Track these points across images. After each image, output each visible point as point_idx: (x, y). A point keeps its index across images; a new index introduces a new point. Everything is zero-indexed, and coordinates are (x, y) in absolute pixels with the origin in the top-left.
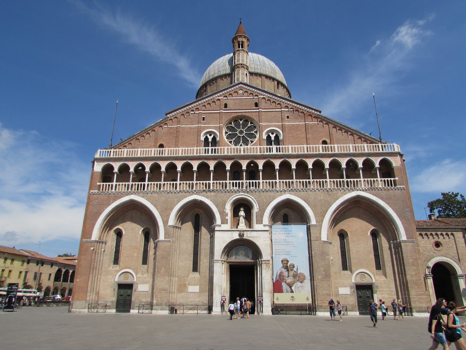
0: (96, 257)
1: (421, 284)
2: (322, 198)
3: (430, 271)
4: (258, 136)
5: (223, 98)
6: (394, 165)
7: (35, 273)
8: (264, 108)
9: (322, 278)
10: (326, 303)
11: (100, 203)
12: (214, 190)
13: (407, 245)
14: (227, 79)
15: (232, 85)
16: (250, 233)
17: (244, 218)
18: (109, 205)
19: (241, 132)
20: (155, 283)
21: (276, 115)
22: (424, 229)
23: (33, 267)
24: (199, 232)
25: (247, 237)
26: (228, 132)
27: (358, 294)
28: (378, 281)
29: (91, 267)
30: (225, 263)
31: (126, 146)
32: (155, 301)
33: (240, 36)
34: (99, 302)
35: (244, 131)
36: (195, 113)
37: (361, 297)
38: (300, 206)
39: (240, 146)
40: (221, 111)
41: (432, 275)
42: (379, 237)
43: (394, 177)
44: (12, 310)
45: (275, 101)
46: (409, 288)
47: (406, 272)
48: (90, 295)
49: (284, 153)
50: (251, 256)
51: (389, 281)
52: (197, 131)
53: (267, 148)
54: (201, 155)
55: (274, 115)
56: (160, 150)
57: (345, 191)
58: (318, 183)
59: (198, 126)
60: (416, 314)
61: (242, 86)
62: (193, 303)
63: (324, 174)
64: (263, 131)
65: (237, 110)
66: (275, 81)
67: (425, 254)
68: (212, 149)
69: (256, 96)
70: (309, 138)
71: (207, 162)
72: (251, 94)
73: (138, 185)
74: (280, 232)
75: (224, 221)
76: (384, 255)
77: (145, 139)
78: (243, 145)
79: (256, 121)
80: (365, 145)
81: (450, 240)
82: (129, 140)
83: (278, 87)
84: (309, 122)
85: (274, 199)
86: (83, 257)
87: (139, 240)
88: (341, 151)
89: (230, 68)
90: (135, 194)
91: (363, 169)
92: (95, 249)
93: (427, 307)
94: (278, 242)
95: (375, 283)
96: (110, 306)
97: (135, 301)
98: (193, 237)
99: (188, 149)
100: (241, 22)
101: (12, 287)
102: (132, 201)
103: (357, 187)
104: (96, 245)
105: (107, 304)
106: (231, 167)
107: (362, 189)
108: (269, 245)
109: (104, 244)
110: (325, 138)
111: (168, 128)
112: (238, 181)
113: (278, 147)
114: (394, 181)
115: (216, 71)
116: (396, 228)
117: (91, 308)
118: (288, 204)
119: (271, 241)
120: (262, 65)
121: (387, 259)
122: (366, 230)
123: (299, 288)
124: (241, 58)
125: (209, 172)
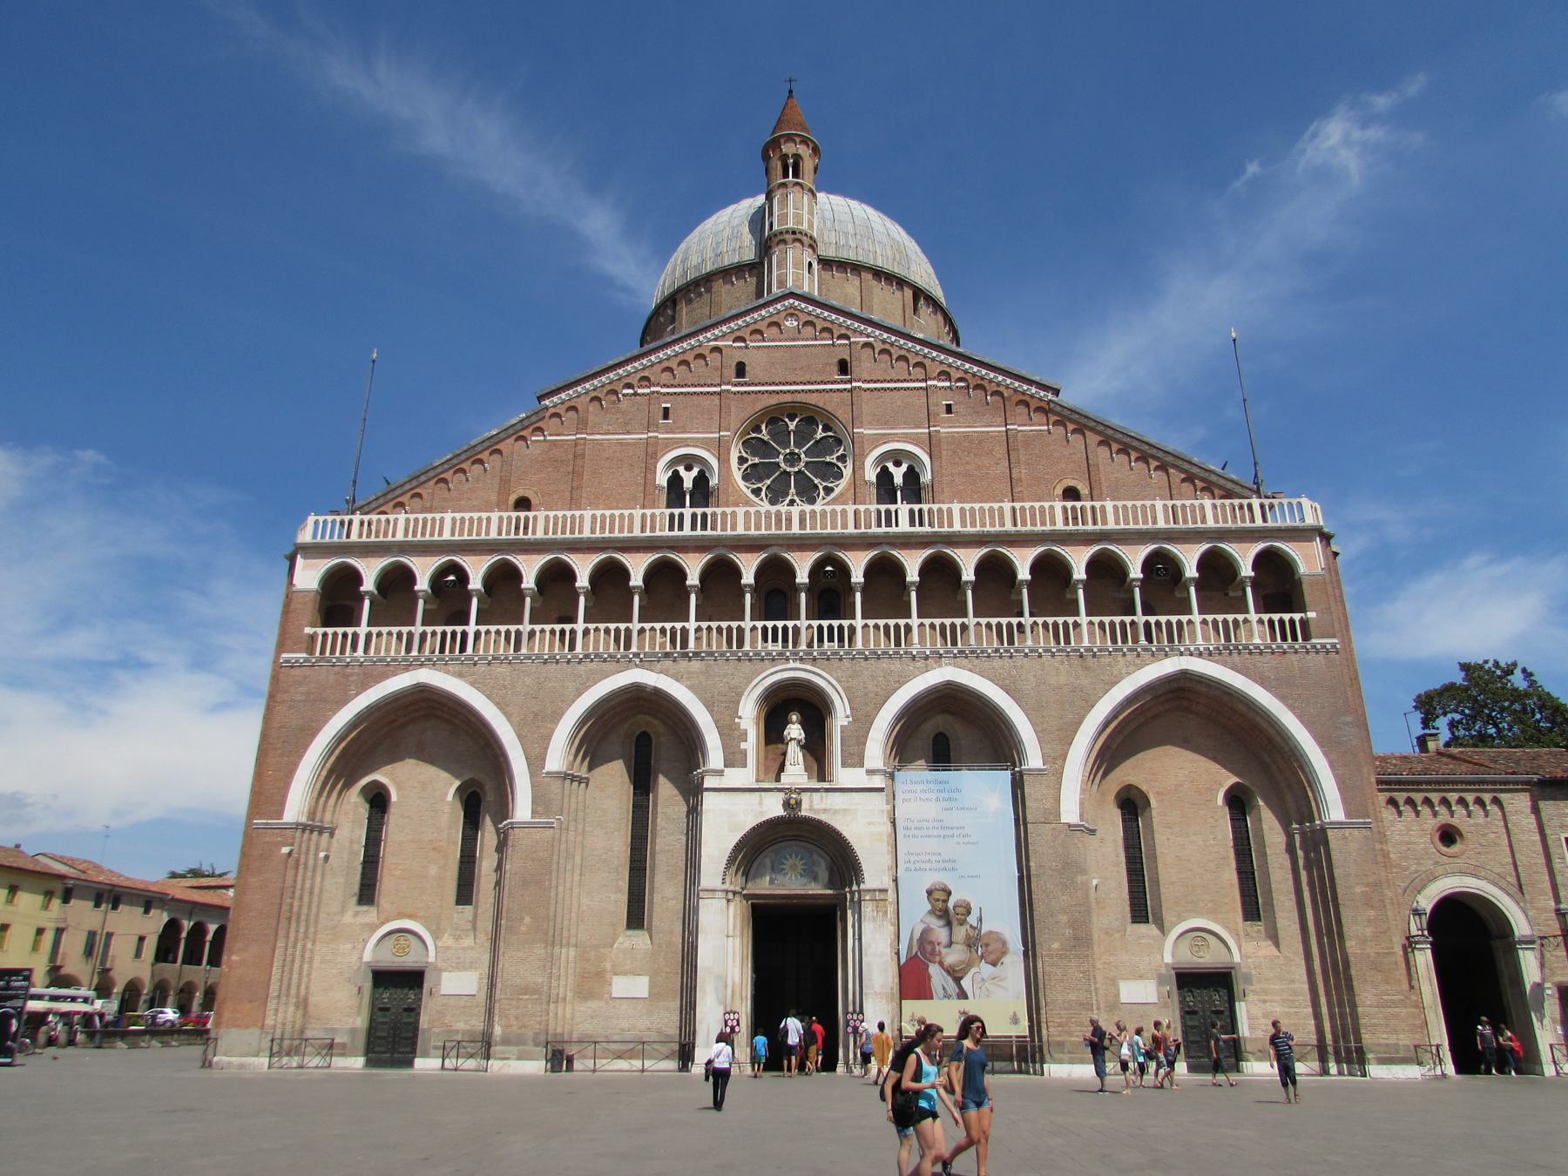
0: (300, 878)
1: (1395, 967)
2: (1063, 680)
3: (1425, 926)
4: (847, 472)
5: (731, 343)
6: (1302, 569)
7: (90, 932)
8: (869, 379)
9: (1062, 949)
10: (1076, 1033)
11: (312, 697)
12: (701, 652)
13: (1345, 838)
14: (746, 281)
15: (761, 301)
16: (822, 798)
17: (803, 747)
18: (343, 701)
19: (793, 459)
20: (500, 966)
21: (909, 400)
22: (1401, 784)
23: (84, 915)
24: (651, 795)
25: (811, 810)
26: (749, 457)
27: (1182, 1002)
28: (1249, 957)
29: (280, 912)
30: (738, 898)
31: (402, 505)
32: (500, 1028)
33: (790, 138)
34: (309, 1034)
35: (803, 456)
36: (636, 394)
37: (1195, 1013)
38: (988, 707)
39: (788, 505)
40: (724, 387)
41: (1431, 939)
42: (1255, 811)
43: (1303, 609)
44: (9, 1060)
45: (907, 355)
46: (1355, 983)
47: (1345, 929)
48: (277, 1010)
49: (936, 529)
50: (824, 875)
51: (1286, 957)
52: (643, 455)
53: (879, 512)
54: (658, 533)
55: (902, 402)
56: (518, 519)
57: (1138, 656)
58: (1048, 631)
59: (645, 436)
60: (1376, 1071)
61: (797, 303)
62: (628, 1036)
63: (1069, 599)
64: (868, 454)
65: (777, 384)
66: (905, 288)
67: (1408, 868)
68: (694, 516)
69: (841, 337)
70: (1020, 480)
71: (677, 558)
72: (824, 330)
73: (444, 634)
74: (924, 796)
75: (734, 759)
76: (1271, 870)
77: (467, 480)
78: (798, 501)
79: (844, 422)
80: (1208, 503)
81: (1489, 819)
82: (415, 483)
83: (915, 310)
84: (1019, 426)
85: (901, 684)
86: (254, 880)
87: (444, 820)
88: (1126, 522)
89: (754, 243)
90: (434, 665)
91: (1200, 584)
92: (294, 852)
93: (1416, 1046)
94: (916, 828)
95: (1239, 964)
96: (344, 1046)
97: (429, 1029)
98: (628, 810)
99: (612, 516)
100: (791, 92)
101: (8, 982)
102: (422, 691)
103: (1179, 642)
104: (297, 840)
105: (333, 1040)
106: (758, 576)
107: (1195, 648)
108: (885, 838)
109: (326, 836)
110: (1073, 479)
111: (547, 444)
112: (780, 624)
113: (916, 507)
114: (1304, 623)
115: (710, 254)
116: (1309, 782)
117: (279, 1054)
118: (949, 699)
119: (894, 823)
120: (862, 233)
121: (1279, 883)
122: (1208, 786)
123: (987, 985)
124: (791, 210)
125: (684, 593)
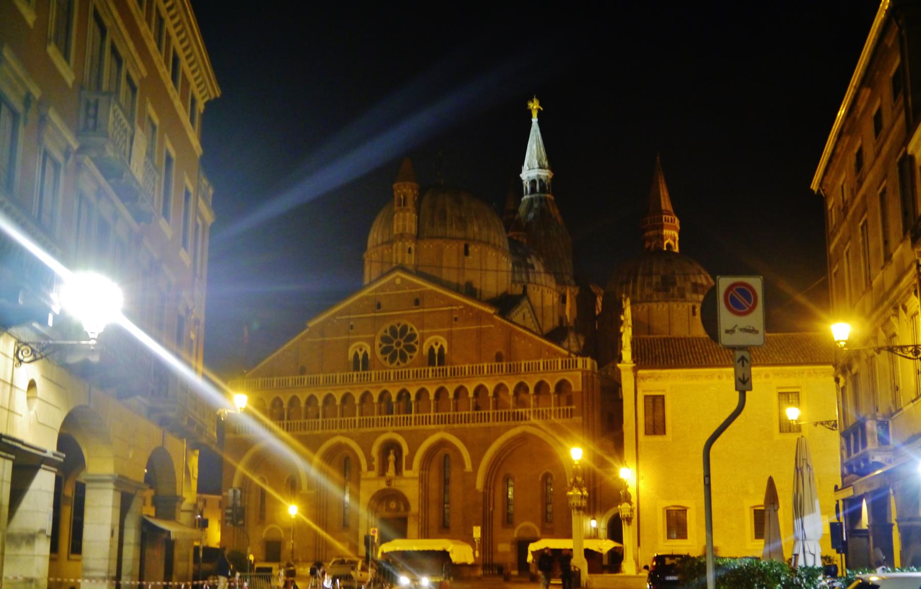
4: (418, 349)
6: (574, 389)
19: (398, 344)
35: (402, 342)
83: (467, 253)
114: (571, 410)
